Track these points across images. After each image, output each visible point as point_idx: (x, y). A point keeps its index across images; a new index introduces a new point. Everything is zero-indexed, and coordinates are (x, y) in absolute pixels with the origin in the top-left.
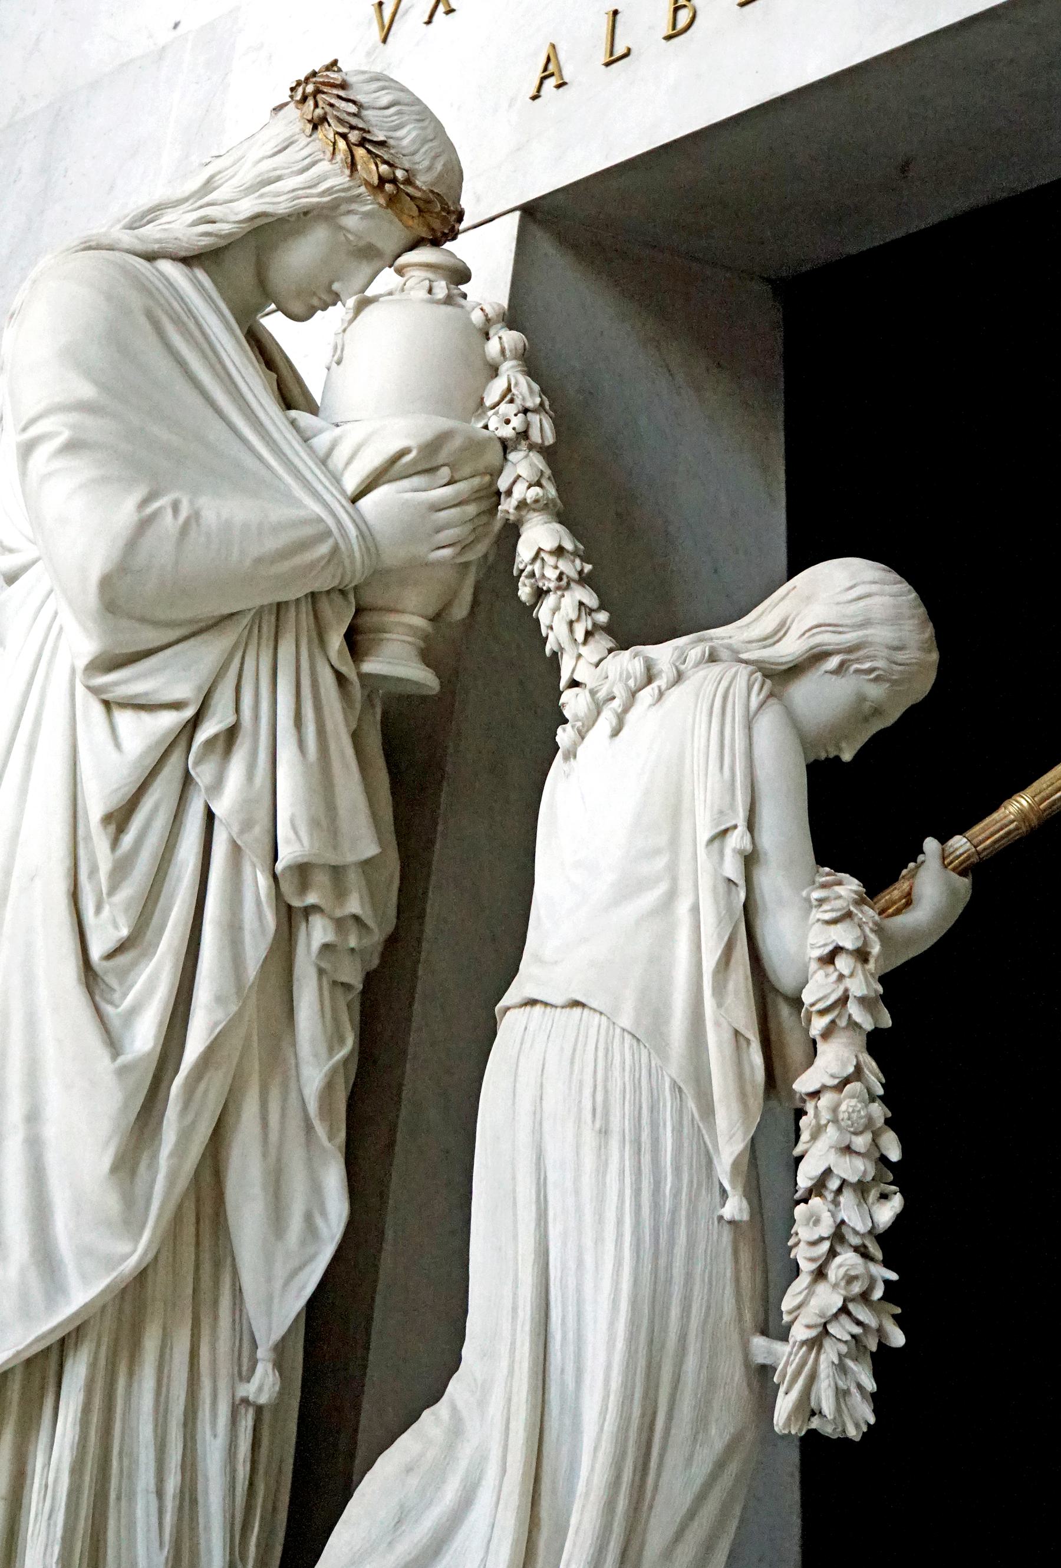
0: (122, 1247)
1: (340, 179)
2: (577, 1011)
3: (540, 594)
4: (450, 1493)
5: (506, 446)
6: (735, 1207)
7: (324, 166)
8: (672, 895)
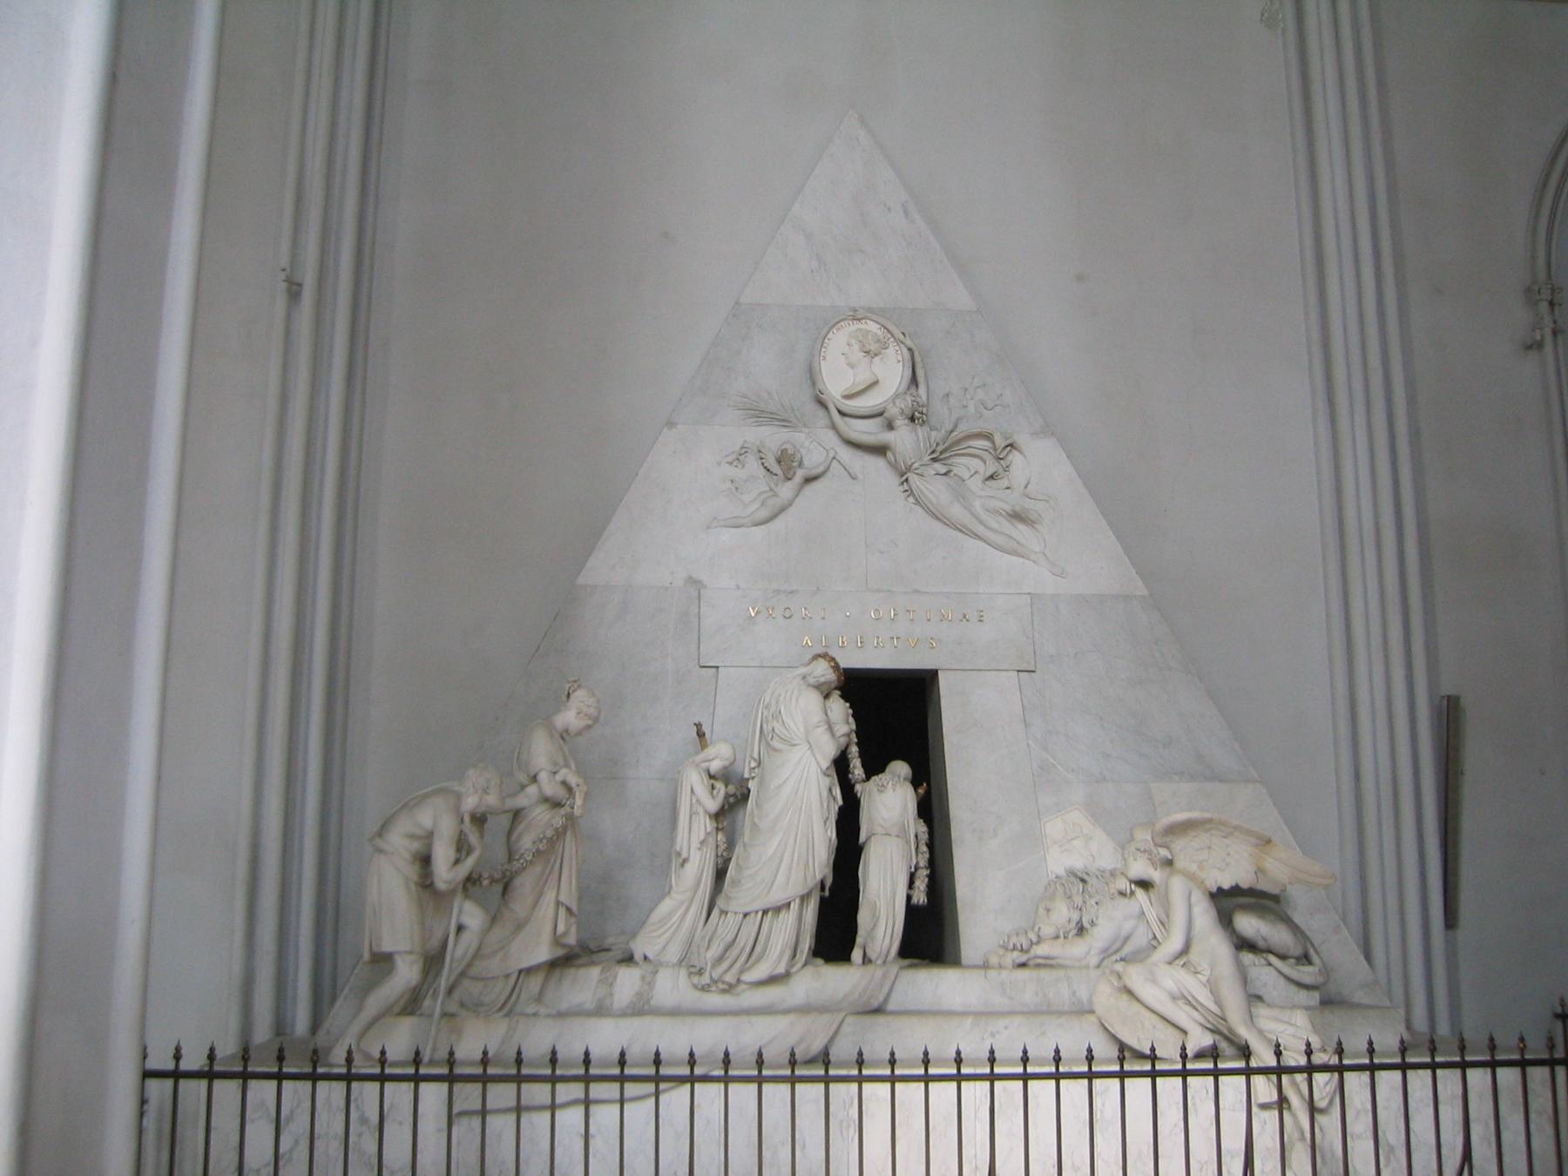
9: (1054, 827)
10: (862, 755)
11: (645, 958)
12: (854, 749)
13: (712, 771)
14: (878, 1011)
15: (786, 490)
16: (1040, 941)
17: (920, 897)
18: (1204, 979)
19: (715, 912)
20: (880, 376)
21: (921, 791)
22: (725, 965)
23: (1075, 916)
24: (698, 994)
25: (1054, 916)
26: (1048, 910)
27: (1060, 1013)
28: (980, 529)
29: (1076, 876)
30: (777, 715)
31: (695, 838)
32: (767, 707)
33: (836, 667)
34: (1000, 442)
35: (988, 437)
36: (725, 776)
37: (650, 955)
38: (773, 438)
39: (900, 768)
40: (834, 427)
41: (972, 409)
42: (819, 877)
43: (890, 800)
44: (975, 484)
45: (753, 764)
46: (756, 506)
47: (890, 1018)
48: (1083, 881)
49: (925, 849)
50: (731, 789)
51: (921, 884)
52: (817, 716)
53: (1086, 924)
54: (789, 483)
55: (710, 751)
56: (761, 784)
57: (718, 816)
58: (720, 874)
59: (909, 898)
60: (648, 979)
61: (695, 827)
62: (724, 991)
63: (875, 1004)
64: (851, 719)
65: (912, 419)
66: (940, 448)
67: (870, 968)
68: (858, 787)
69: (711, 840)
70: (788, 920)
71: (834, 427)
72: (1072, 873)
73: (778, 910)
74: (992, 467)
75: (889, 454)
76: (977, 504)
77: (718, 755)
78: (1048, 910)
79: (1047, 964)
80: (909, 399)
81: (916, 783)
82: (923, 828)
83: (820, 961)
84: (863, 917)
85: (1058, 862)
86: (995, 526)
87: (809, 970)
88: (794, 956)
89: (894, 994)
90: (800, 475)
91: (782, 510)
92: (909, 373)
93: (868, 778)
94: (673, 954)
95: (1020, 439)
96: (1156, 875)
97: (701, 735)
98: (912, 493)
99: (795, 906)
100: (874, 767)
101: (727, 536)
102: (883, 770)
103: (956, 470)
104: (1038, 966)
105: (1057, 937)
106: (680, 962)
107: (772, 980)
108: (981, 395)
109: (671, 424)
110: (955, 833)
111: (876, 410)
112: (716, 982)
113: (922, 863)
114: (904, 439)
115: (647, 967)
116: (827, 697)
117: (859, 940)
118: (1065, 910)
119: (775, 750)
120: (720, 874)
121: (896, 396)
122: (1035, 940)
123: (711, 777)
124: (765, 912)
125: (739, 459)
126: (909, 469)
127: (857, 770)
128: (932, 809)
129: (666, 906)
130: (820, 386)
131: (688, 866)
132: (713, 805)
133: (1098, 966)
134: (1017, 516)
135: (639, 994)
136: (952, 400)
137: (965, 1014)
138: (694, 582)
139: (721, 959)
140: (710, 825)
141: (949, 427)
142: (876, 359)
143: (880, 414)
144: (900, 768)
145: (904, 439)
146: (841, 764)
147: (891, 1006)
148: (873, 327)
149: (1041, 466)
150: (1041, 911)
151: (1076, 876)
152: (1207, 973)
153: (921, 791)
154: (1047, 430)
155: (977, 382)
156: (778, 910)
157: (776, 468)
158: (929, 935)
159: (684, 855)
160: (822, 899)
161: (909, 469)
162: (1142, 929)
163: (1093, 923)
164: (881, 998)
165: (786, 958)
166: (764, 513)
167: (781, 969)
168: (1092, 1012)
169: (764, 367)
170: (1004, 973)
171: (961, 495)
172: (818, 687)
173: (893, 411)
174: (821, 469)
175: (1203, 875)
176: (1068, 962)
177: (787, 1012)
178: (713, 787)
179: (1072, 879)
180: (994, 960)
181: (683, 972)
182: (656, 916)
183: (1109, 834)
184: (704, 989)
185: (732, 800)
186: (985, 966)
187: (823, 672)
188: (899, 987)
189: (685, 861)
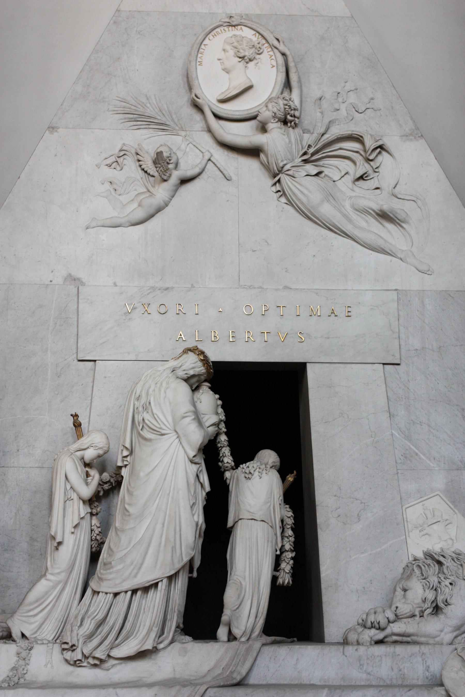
0: (192, 552)
1: (204, 371)
2: (262, 522)
3: (222, 447)
4: (243, 594)
5: (221, 421)
6: (278, 553)
7: (203, 368)
8: (270, 505)
9: (414, 513)
10: (231, 444)
11: (23, 635)
12: (223, 438)
13: (87, 459)
14: (240, 684)
15: (162, 192)
16: (398, 618)
17: (285, 578)
19: (89, 592)
20: (254, 83)
21: (290, 478)
22: (96, 641)
23: (430, 595)
24: (71, 668)
25: (410, 594)
26: (405, 590)
27: (411, 687)
28: (348, 228)
29: (433, 558)
30: (147, 407)
31: (70, 523)
32: (138, 399)
33: (205, 361)
34: (370, 143)
35: (358, 139)
36: (99, 464)
37: (27, 634)
38: (150, 142)
39: (269, 457)
40: (209, 130)
41: (343, 112)
42: (186, 559)
43: (258, 489)
44: (345, 185)
45: (125, 453)
46: (134, 205)
47: (249, 691)
48: (440, 563)
49: (290, 532)
50: (106, 476)
51: (286, 566)
52: (185, 407)
53: (441, 605)
54: (165, 184)
55: (84, 441)
56: (132, 473)
57: (91, 501)
58: (94, 557)
59: (274, 579)
60: (24, 654)
61: (69, 511)
62: (95, 665)
63: (238, 678)
64: (220, 410)
65: (285, 122)
66: (311, 150)
67: (234, 643)
68: (228, 475)
69: (85, 525)
70: (156, 599)
71: (209, 130)
72: (429, 555)
73: (146, 589)
74: (363, 168)
75: (262, 156)
76: (347, 205)
77: (93, 443)
78: (405, 590)
79: (404, 640)
80: (281, 102)
81: (283, 472)
82: (288, 513)
83: (188, 638)
84: (230, 596)
85: (417, 547)
86: (363, 224)
87: (177, 645)
88: (162, 633)
89: (255, 669)
90: (176, 176)
91: (159, 210)
92: (282, 77)
93: (237, 466)
94: (49, 632)
95: (388, 142)
97: (77, 425)
98: (284, 194)
99: (162, 586)
100: (243, 456)
101: (108, 236)
102: (251, 458)
103: (326, 171)
104: (395, 642)
105: (413, 616)
106: (55, 640)
107: (141, 655)
108: (352, 98)
109: (52, 129)
110: (321, 518)
111: (252, 113)
112: (86, 657)
113: (287, 547)
114: (277, 141)
115: (24, 643)
116: (195, 389)
117: (225, 618)
119: (146, 439)
120: (94, 557)
121: (270, 100)
122: (392, 617)
123: (86, 465)
124: (134, 592)
125: (117, 161)
126: (281, 170)
127: (227, 459)
128: (299, 496)
129: (42, 586)
130: (196, 91)
131: (62, 549)
132: (87, 491)
133: (451, 644)
134: (384, 216)
135: (14, 669)
136: (325, 104)
137: (323, 687)
138: (72, 279)
139: (91, 636)
140: (84, 510)
141: (322, 130)
142: (251, 64)
143: (254, 118)
144: (269, 457)
145: (277, 141)
146: (209, 451)
147: (252, 680)
148: (247, 33)
149: (410, 168)
150: (399, 592)
151: (433, 558)
153: (290, 478)
154: (416, 134)
155: (349, 86)
156: (146, 589)
157: (152, 170)
158: (295, 612)
159: (59, 539)
160: (191, 582)
161: (281, 170)
163: (447, 603)
164: (244, 672)
165: (153, 635)
166: (140, 214)
167: (149, 646)
168: (442, 685)
169: (144, 74)
170: (362, 649)
171: (330, 196)
172: (186, 380)
173: (266, 114)
174: (197, 170)
176: (423, 639)
177: (150, 685)
178: (88, 475)
179: (429, 561)
180: (352, 637)
181: (57, 648)
182: (32, 596)
184: (76, 664)
185: (106, 487)
186: (345, 642)
187: (193, 365)
188: (263, 661)
189: (60, 543)
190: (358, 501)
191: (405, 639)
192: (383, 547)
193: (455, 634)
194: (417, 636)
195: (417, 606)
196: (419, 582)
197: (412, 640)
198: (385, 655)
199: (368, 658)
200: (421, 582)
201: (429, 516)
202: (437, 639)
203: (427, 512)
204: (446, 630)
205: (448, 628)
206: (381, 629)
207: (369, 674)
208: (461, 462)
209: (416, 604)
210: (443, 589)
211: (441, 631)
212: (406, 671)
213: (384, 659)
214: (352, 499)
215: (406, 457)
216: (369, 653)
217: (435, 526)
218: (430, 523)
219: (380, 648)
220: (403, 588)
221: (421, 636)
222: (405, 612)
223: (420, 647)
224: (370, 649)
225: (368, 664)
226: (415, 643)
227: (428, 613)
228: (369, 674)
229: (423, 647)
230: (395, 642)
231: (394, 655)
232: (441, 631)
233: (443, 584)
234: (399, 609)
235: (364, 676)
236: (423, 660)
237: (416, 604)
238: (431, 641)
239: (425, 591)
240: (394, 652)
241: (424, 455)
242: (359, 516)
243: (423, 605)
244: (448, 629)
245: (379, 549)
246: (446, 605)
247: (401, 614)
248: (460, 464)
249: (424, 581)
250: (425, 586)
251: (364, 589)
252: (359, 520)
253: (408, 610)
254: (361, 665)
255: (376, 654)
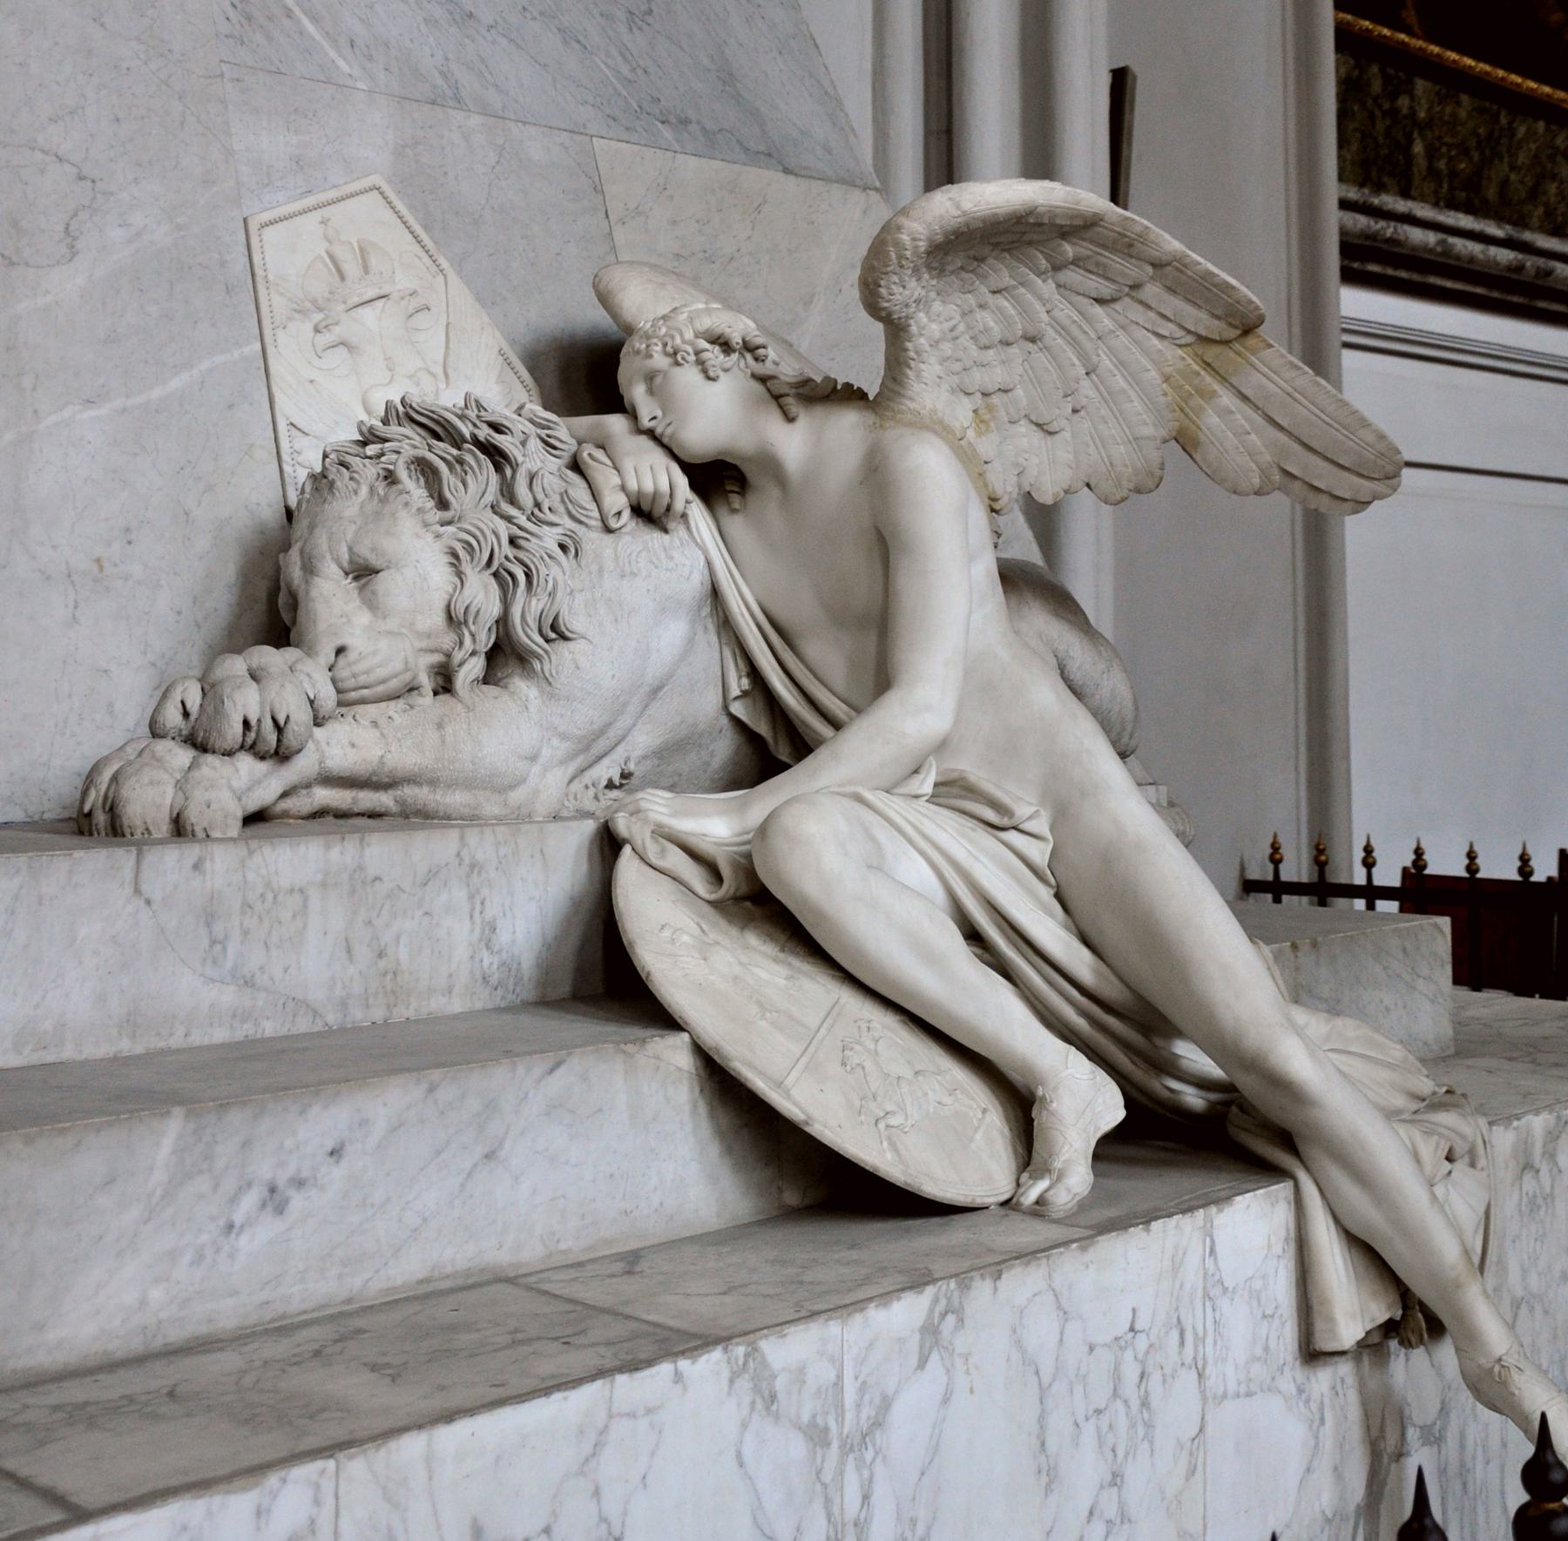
9: (291, 254)
18: (1039, 853)
78: (362, 572)
96: (791, 442)
118: (439, 576)
122: (327, 696)
152: (1041, 826)
162: (710, 652)
175: (986, 446)
176: (456, 800)
180: (147, 800)
183: (487, 299)
190: (67, 167)
191: (368, 799)
192: (175, 383)
193: (571, 768)
194: (433, 783)
195: (424, 644)
196: (429, 537)
197: (401, 802)
198: (324, 885)
199: (247, 906)
200: (438, 536)
201: (352, 268)
202: (516, 796)
203: (342, 254)
204: (546, 753)
205: (555, 742)
206: (281, 755)
207: (249, 983)
208: (442, 73)
209: (419, 635)
210: (543, 571)
211: (533, 758)
212: (403, 954)
213: (315, 904)
214: (39, 156)
215: (249, 18)
216: (251, 876)
217: (367, 313)
218: (356, 300)
219: (302, 848)
220: (351, 562)
221: (452, 785)
222: (381, 673)
223: (462, 838)
224: (257, 858)
225: (246, 933)
226: (416, 817)
227: (472, 677)
228: (249, 983)
229: (473, 836)
230: (319, 814)
231: (359, 882)
232: (533, 758)
233: (532, 545)
234: (352, 655)
235: (228, 996)
236: (471, 897)
237: (419, 635)
238: (492, 807)
239: (460, 574)
240: (361, 868)
241: (315, 20)
242: (70, 237)
243: (447, 641)
244: (555, 748)
245: (157, 393)
246: (548, 641)
247: (363, 679)
248: (440, 81)
249: (451, 529)
250: (462, 553)
251: (101, 568)
252: (74, 253)
253: (398, 665)
254: (213, 942)
255: (285, 882)
